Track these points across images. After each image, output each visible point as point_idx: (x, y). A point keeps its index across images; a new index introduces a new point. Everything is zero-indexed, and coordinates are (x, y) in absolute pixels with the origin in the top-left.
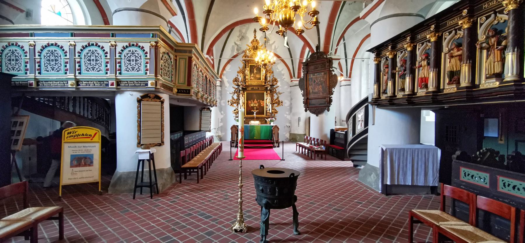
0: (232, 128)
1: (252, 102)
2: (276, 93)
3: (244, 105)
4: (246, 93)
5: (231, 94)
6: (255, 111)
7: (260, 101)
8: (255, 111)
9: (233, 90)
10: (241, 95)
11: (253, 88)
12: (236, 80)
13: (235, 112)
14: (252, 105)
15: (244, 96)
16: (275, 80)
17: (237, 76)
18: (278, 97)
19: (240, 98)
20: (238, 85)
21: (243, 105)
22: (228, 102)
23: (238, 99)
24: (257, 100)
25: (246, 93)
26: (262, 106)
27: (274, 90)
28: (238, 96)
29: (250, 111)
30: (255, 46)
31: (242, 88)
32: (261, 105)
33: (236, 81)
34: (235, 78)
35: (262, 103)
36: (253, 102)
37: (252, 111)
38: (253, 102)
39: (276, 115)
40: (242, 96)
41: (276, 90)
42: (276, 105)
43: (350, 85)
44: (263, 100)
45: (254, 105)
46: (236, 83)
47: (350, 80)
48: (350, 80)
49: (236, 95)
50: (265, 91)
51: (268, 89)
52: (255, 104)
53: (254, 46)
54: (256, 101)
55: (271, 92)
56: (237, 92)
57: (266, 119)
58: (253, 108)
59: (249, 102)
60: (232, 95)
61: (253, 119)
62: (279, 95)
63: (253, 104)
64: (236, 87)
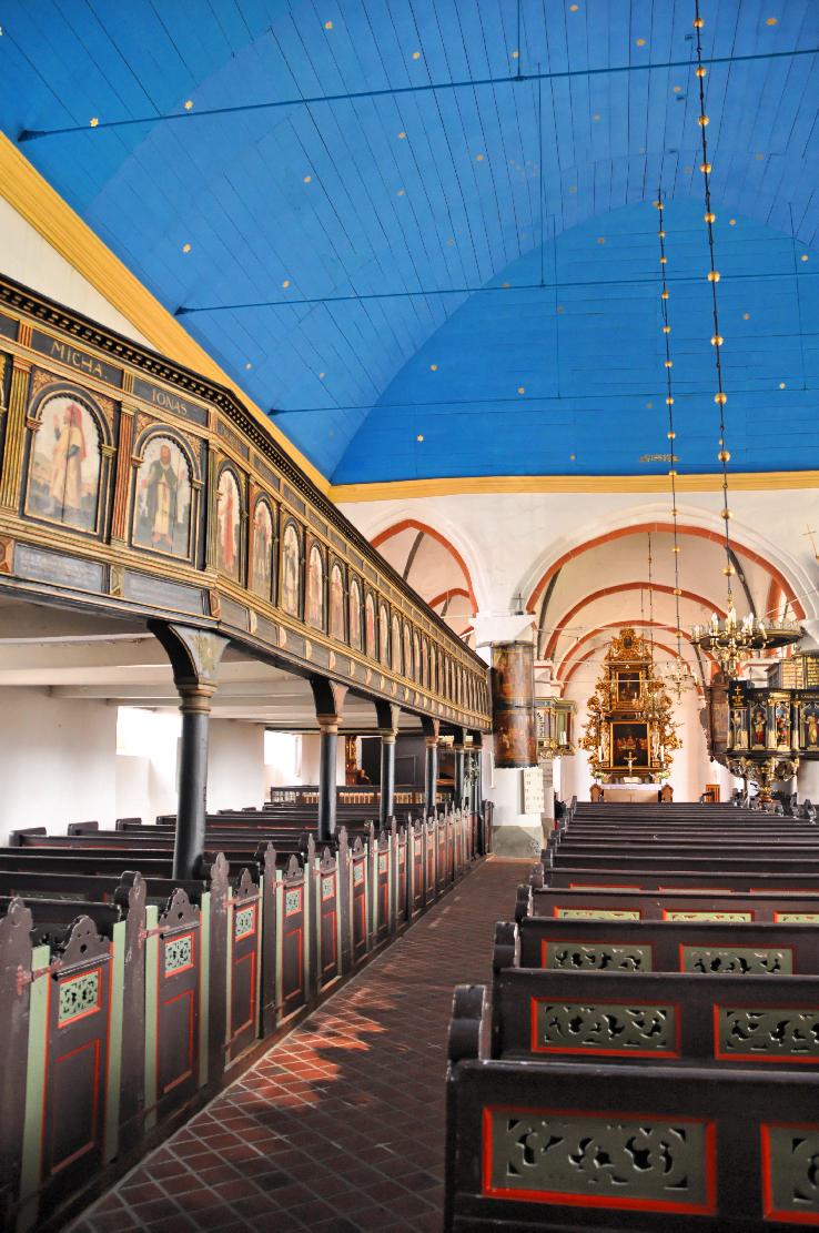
0: (592, 789)
5: (584, 727)
9: (587, 720)
10: (603, 730)
12: (592, 701)
14: (624, 748)
20: (597, 710)
24: (633, 738)
29: (621, 758)
31: (606, 717)
39: (670, 765)
42: (669, 747)
44: (645, 737)
49: (593, 728)
53: (625, 639)
54: (631, 740)
56: (596, 723)
58: (626, 753)
60: (585, 730)
61: (626, 773)
62: (676, 729)
64: (594, 714)
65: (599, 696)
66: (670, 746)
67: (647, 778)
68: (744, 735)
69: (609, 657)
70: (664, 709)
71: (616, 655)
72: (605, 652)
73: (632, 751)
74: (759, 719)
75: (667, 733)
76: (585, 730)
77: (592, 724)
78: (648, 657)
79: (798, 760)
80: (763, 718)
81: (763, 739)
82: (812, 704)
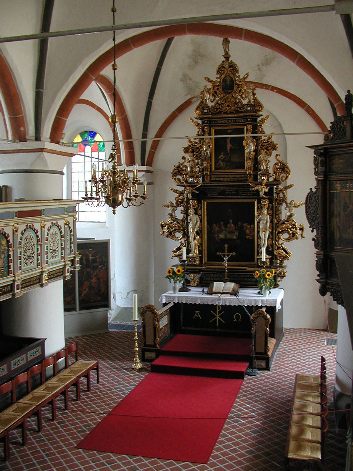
1: (223, 228)
2: (286, 203)
5: (168, 207)
6: (226, 253)
7: (242, 227)
8: (226, 253)
9: (172, 197)
10: (191, 212)
11: (224, 191)
12: (179, 171)
14: (222, 236)
16: (283, 169)
18: (291, 216)
22: (162, 226)
24: (235, 224)
26: (248, 237)
27: (281, 195)
28: (186, 213)
30: (228, 79)
32: (246, 235)
33: (181, 174)
34: (177, 164)
36: (226, 227)
37: (218, 253)
38: (226, 227)
39: (285, 263)
41: (284, 196)
45: (228, 237)
50: (255, 198)
51: (262, 194)
52: (231, 232)
53: (224, 81)
55: (271, 202)
59: (216, 228)
63: (224, 232)
66: (286, 236)
69: (202, 107)
70: (277, 181)
71: (211, 104)
75: (283, 217)
76: (169, 210)
78: (257, 106)
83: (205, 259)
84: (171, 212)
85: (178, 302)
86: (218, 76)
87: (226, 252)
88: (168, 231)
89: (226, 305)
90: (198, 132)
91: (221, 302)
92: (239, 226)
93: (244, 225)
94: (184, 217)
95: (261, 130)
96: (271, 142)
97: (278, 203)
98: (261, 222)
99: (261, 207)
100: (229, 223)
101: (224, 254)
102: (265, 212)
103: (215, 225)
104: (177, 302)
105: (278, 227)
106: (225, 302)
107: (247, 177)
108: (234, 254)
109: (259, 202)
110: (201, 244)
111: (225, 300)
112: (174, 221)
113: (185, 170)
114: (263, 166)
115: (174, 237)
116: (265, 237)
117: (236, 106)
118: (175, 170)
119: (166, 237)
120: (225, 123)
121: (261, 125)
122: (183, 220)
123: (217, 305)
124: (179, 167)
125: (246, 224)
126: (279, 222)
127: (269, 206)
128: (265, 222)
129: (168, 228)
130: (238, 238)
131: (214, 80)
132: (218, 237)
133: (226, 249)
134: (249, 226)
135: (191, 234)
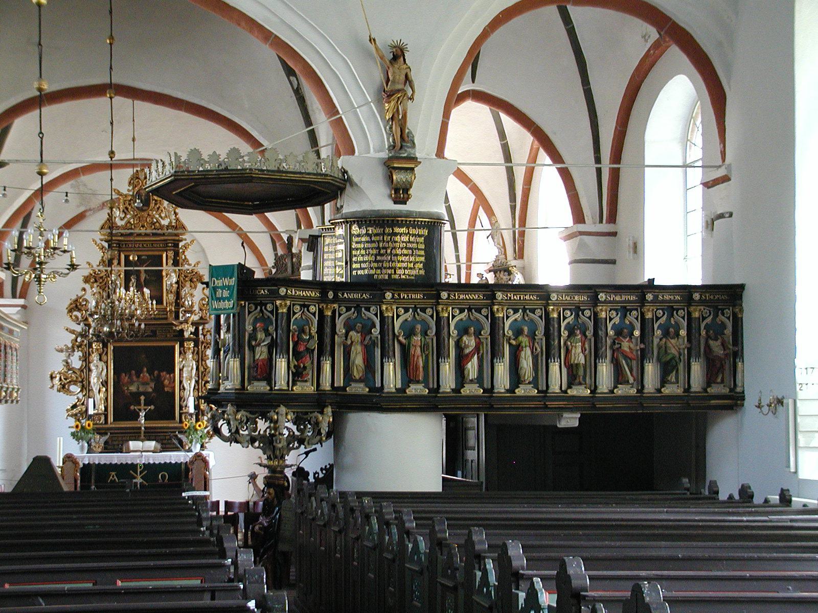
1: (135, 378)
3: (107, 390)
4: (111, 348)
5: (61, 351)
7: (159, 376)
9: (67, 339)
10: (95, 357)
12: (76, 305)
13: (75, 411)
14: (133, 388)
15: (104, 358)
17: (81, 293)
19: (92, 367)
21: (104, 389)
22: (52, 378)
23: (86, 368)
24: (150, 372)
25: (111, 348)
26: (166, 389)
28: (86, 359)
32: (164, 386)
33: (79, 310)
34: (74, 297)
35: (166, 382)
36: (138, 376)
38: (138, 376)
40: (100, 360)
43: (613, 262)
45: (141, 389)
46: (78, 314)
47: (614, 234)
48: (614, 234)
49: (78, 354)
50: (176, 341)
51: (186, 335)
52: (145, 384)
54: (145, 375)
55: (196, 345)
56: (82, 343)
57: (180, 436)
58: (136, 396)
59: (125, 378)
60: (63, 356)
61: (136, 435)
63: (136, 384)
65: (88, 296)
67: (168, 442)
68: (233, 364)
71: (120, 223)
72: (103, 216)
73: (144, 393)
74: (260, 335)
76: (63, 356)
77: (75, 346)
79: (329, 410)
80: (267, 333)
81: (266, 372)
82: (358, 308)
83: (111, 418)
84: (65, 358)
85: (89, 463)
86: (131, 188)
87: (142, 405)
88: (61, 384)
89: (149, 463)
90: (103, 257)
91: (143, 459)
92: (155, 375)
93: (162, 374)
94: (82, 365)
95: (183, 257)
96: (196, 273)
97: (205, 347)
98: (185, 369)
99: (184, 351)
100: (141, 371)
101: (139, 407)
102: (191, 356)
103: (124, 375)
104: (87, 463)
105: (205, 375)
106: (148, 460)
107: (167, 314)
108: (152, 407)
109: (182, 345)
110: (107, 399)
111: (148, 457)
112: (69, 370)
113: (85, 305)
114: (188, 301)
115: (68, 392)
116: (190, 387)
117: (153, 227)
118: (71, 304)
119: (58, 391)
120: (139, 247)
121: (184, 252)
122: (81, 370)
123: (137, 464)
124: (76, 300)
125: (164, 373)
126: (206, 369)
127: (194, 350)
128: (190, 369)
129: (60, 379)
130: (155, 390)
131: (125, 192)
132: (128, 389)
133: (142, 402)
134: (168, 376)
135: (94, 385)
